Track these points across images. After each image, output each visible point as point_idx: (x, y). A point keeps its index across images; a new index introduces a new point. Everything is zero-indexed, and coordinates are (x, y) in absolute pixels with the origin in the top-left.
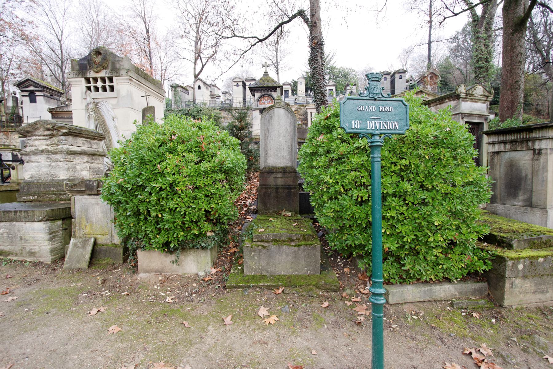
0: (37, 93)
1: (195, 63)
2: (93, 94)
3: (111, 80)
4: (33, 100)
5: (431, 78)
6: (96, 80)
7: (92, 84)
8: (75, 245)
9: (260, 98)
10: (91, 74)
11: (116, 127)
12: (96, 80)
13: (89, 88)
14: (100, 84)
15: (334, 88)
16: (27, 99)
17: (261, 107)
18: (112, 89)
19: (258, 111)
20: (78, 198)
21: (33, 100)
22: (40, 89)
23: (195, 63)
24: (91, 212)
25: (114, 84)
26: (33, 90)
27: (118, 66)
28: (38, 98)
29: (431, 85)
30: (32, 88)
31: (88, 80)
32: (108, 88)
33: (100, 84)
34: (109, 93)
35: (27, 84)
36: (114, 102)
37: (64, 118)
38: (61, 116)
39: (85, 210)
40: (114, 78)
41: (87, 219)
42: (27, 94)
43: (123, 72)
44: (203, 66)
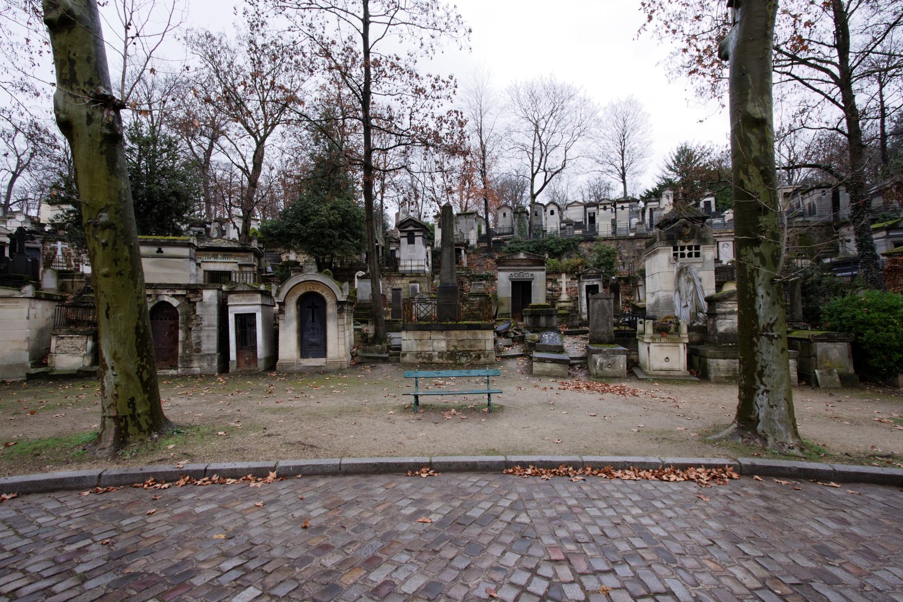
0: (416, 234)
2: (679, 259)
3: (697, 248)
4: (411, 241)
5: (897, 190)
6: (683, 248)
7: (679, 252)
8: (821, 374)
10: (681, 243)
11: (701, 286)
13: (675, 255)
14: (686, 251)
15: (712, 199)
16: (404, 241)
18: (697, 255)
20: (818, 344)
21: (411, 241)
24: (830, 353)
25: (701, 251)
27: (703, 236)
28: (416, 239)
29: (898, 199)
30: (411, 228)
31: (675, 249)
33: (686, 251)
34: (694, 259)
36: (699, 266)
39: (826, 352)
40: (701, 247)
41: (828, 357)
42: (405, 234)
43: (711, 242)
44: (545, 183)
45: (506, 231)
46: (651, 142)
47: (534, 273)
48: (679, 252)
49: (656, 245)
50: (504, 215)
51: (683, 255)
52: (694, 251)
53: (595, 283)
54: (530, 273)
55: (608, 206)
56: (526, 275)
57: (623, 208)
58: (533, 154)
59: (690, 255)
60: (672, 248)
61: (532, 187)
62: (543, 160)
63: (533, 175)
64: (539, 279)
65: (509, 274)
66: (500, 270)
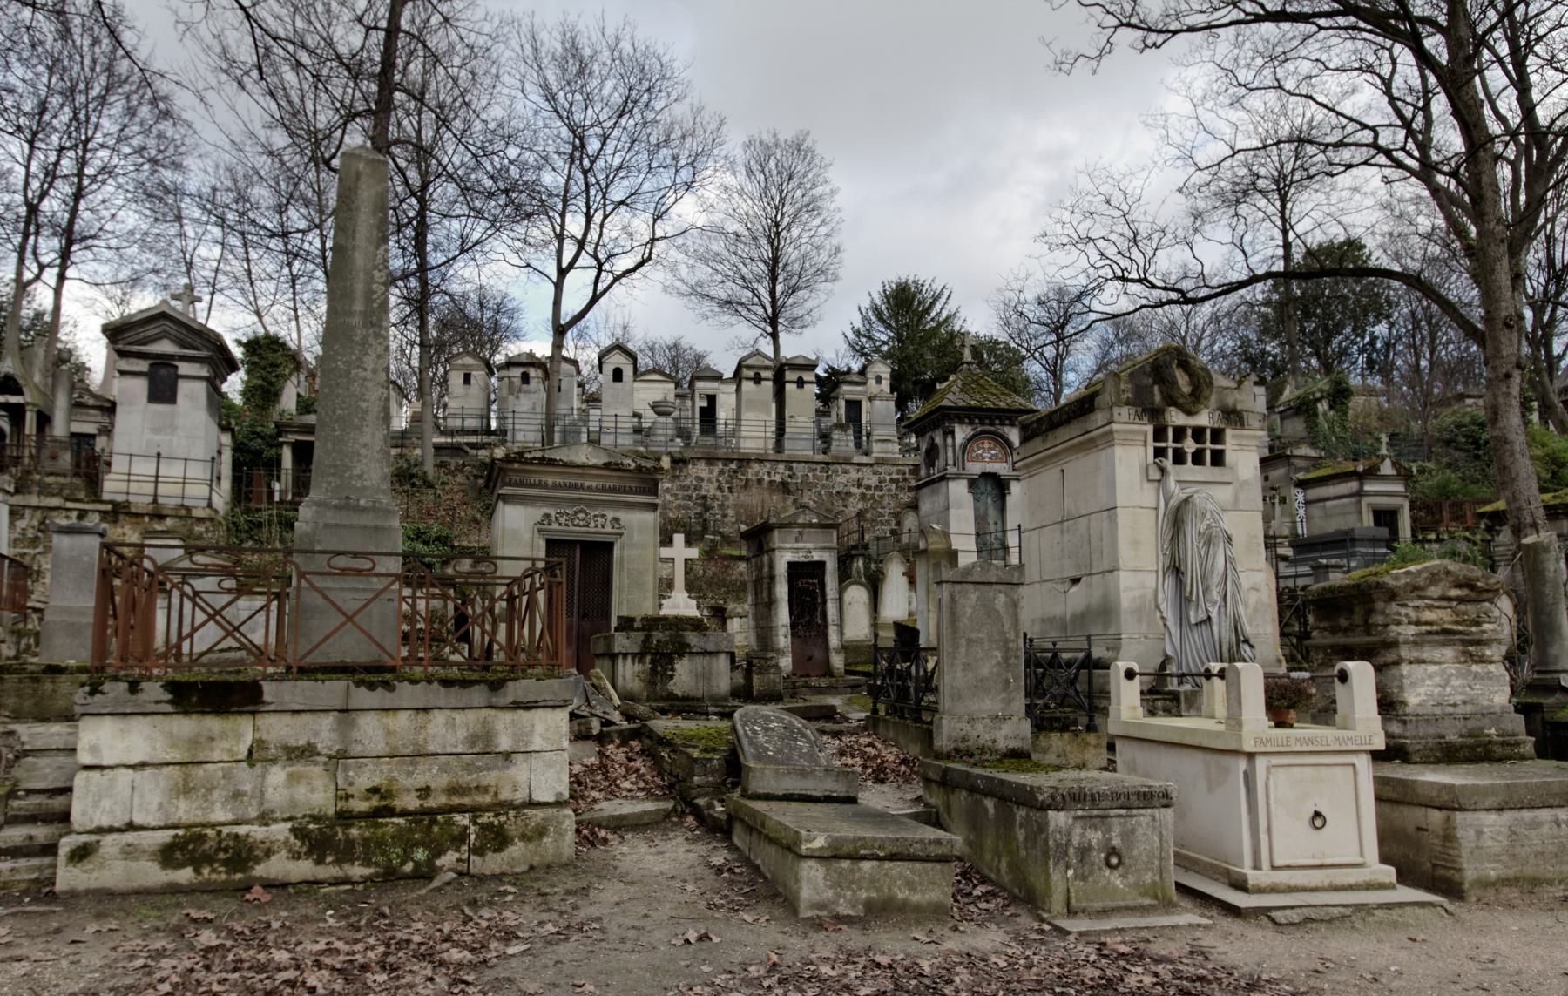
0: (184, 368)
1: (558, 287)
3: (1217, 435)
9: (969, 440)
10: (1176, 418)
12: (1179, 433)
13: (1160, 453)
14: (1190, 446)
17: (975, 468)
18: (1218, 459)
19: (965, 482)
21: (163, 390)
22: (204, 353)
23: (558, 287)
26: (172, 357)
28: (184, 387)
30: (166, 347)
31: (1159, 434)
32: (1208, 453)
34: (1207, 472)
35: (152, 330)
37: (546, 486)
38: (534, 479)
42: (143, 366)
44: (595, 299)
45: (471, 423)
46: (838, 250)
47: (623, 515)
48: (1170, 444)
49: (1099, 418)
50: (467, 379)
51: (1179, 458)
52: (1208, 445)
53: (816, 557)
54: (610, 514)
55: (764, 374)
56: (595, 526)
57: (800, 383)
58: (563, 216)
59: (1198, 459)
60: (1150, 429)
61: (557, 303)
62: (594, 228)
63: (562, 273)
64: (635, 532)
65: (537, 513)
66: (506, 499)
